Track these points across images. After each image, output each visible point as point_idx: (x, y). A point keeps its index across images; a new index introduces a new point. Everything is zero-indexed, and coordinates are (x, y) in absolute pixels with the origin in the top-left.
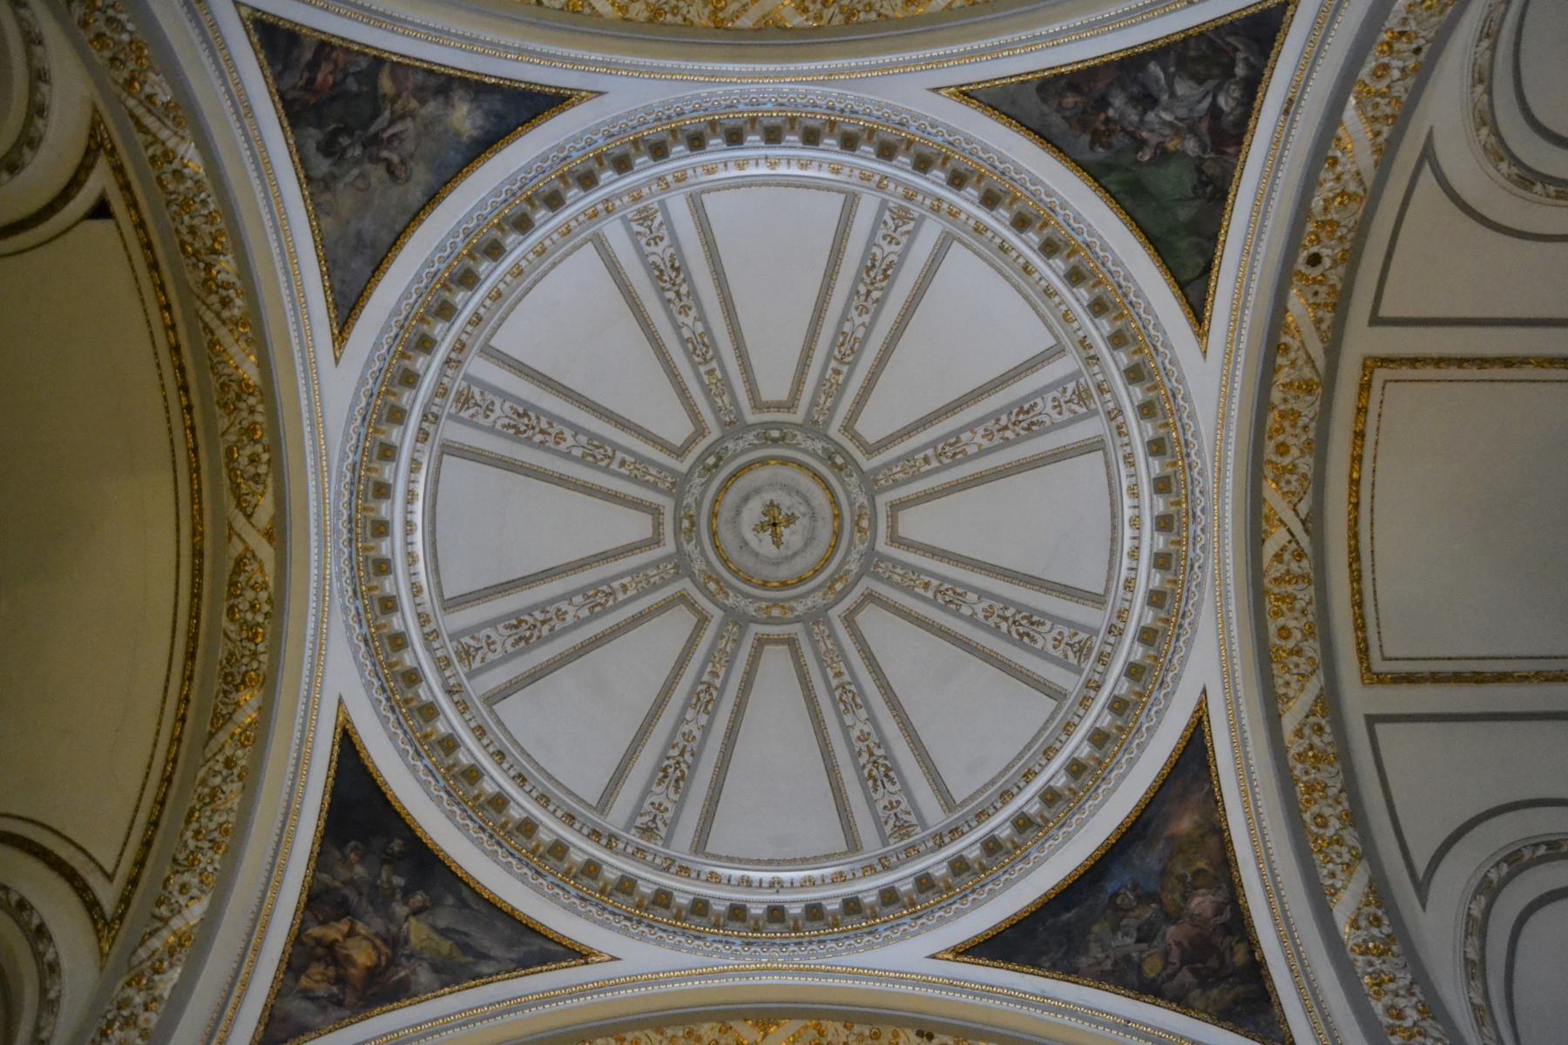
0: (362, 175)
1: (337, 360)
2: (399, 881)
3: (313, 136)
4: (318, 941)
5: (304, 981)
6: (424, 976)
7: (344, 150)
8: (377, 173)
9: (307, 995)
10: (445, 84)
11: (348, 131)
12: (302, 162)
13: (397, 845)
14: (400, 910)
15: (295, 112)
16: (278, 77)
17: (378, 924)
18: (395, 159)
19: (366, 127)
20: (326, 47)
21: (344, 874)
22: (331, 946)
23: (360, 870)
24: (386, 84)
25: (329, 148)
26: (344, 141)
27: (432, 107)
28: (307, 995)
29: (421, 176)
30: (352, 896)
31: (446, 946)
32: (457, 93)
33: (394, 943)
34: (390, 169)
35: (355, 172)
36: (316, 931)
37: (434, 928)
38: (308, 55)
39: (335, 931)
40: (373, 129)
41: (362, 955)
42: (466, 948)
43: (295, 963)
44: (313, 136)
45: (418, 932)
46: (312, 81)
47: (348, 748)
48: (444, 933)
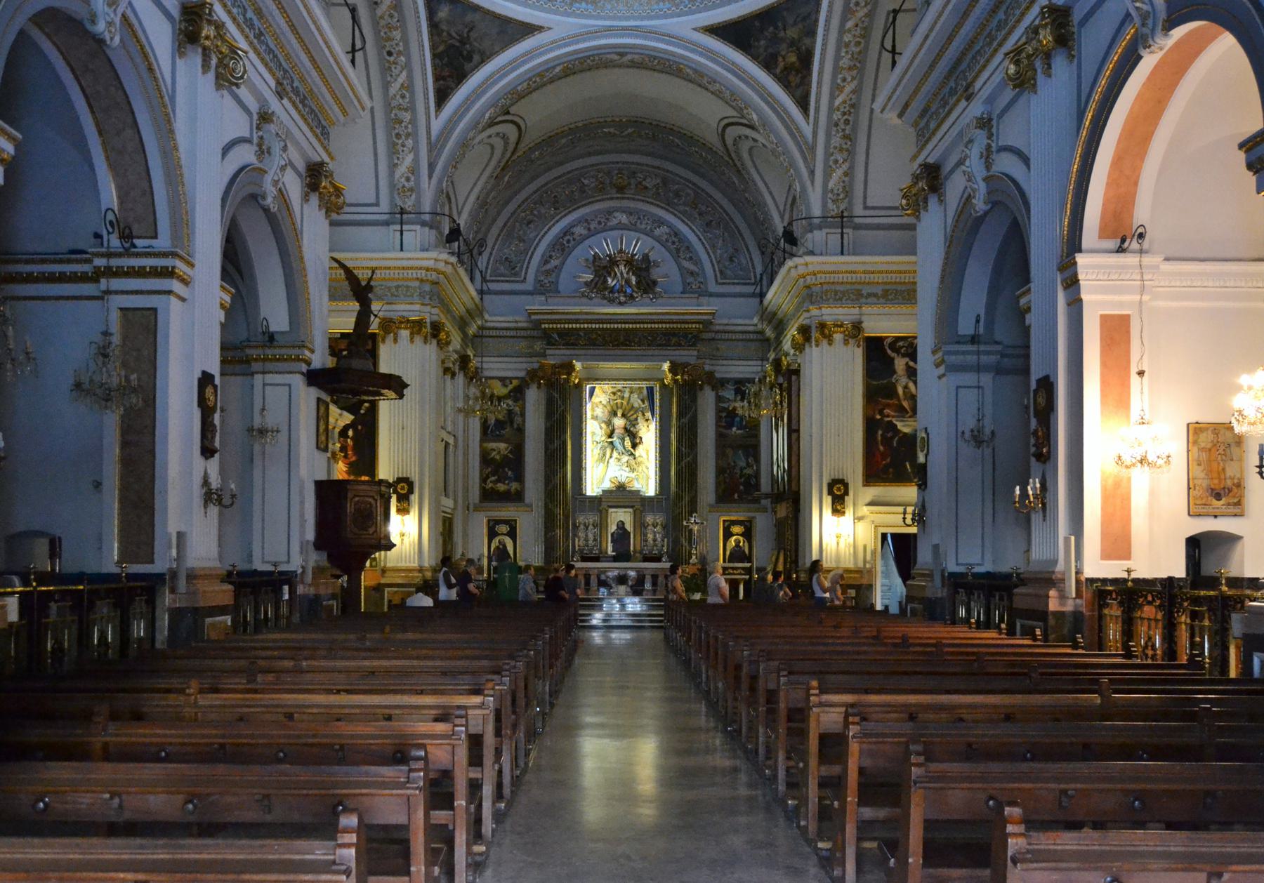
0: (475, 40)
1: (549, 29)
2: (771, 29)
3: (467, 66)
4: (782, 72)
5: (793, 84)
6: (807, 41)
7: (469, 52)
8: (473, 35)
9: (798, 86)
10: (434, 26)
11: (461, 54)
12: (477, 67)
13: (757, 24)
14: (782, 34)
15: (461, 77)
16: (452, 89)
17: (784, 46)
18: (466, 30)
19: (458, 47)
20: (437, 78)
21: (761, 50)
22: (785, 68)
23: (762, 42)
24: (441, 48)
25: (469, 58)
26: (465, 53)
27: (444, 27)
28: (798, 86)
29: (469, 17)
30: (770, 50)
31: (800, 26)
32: (436, 19)
33: (792, 43)
34: (471, 29)
35: (475, 44)
36: (778, 71)
37: (792, 26)
38: (442, 82)
39: (781, 65)
40: (457, 44)
41: (793, 58)
42: (804, 19)
43: (786, 85)
44: (467, 66)
45: (792, 33)
46: (449, 76)
47: (714, 30)
48: (795, 23)
